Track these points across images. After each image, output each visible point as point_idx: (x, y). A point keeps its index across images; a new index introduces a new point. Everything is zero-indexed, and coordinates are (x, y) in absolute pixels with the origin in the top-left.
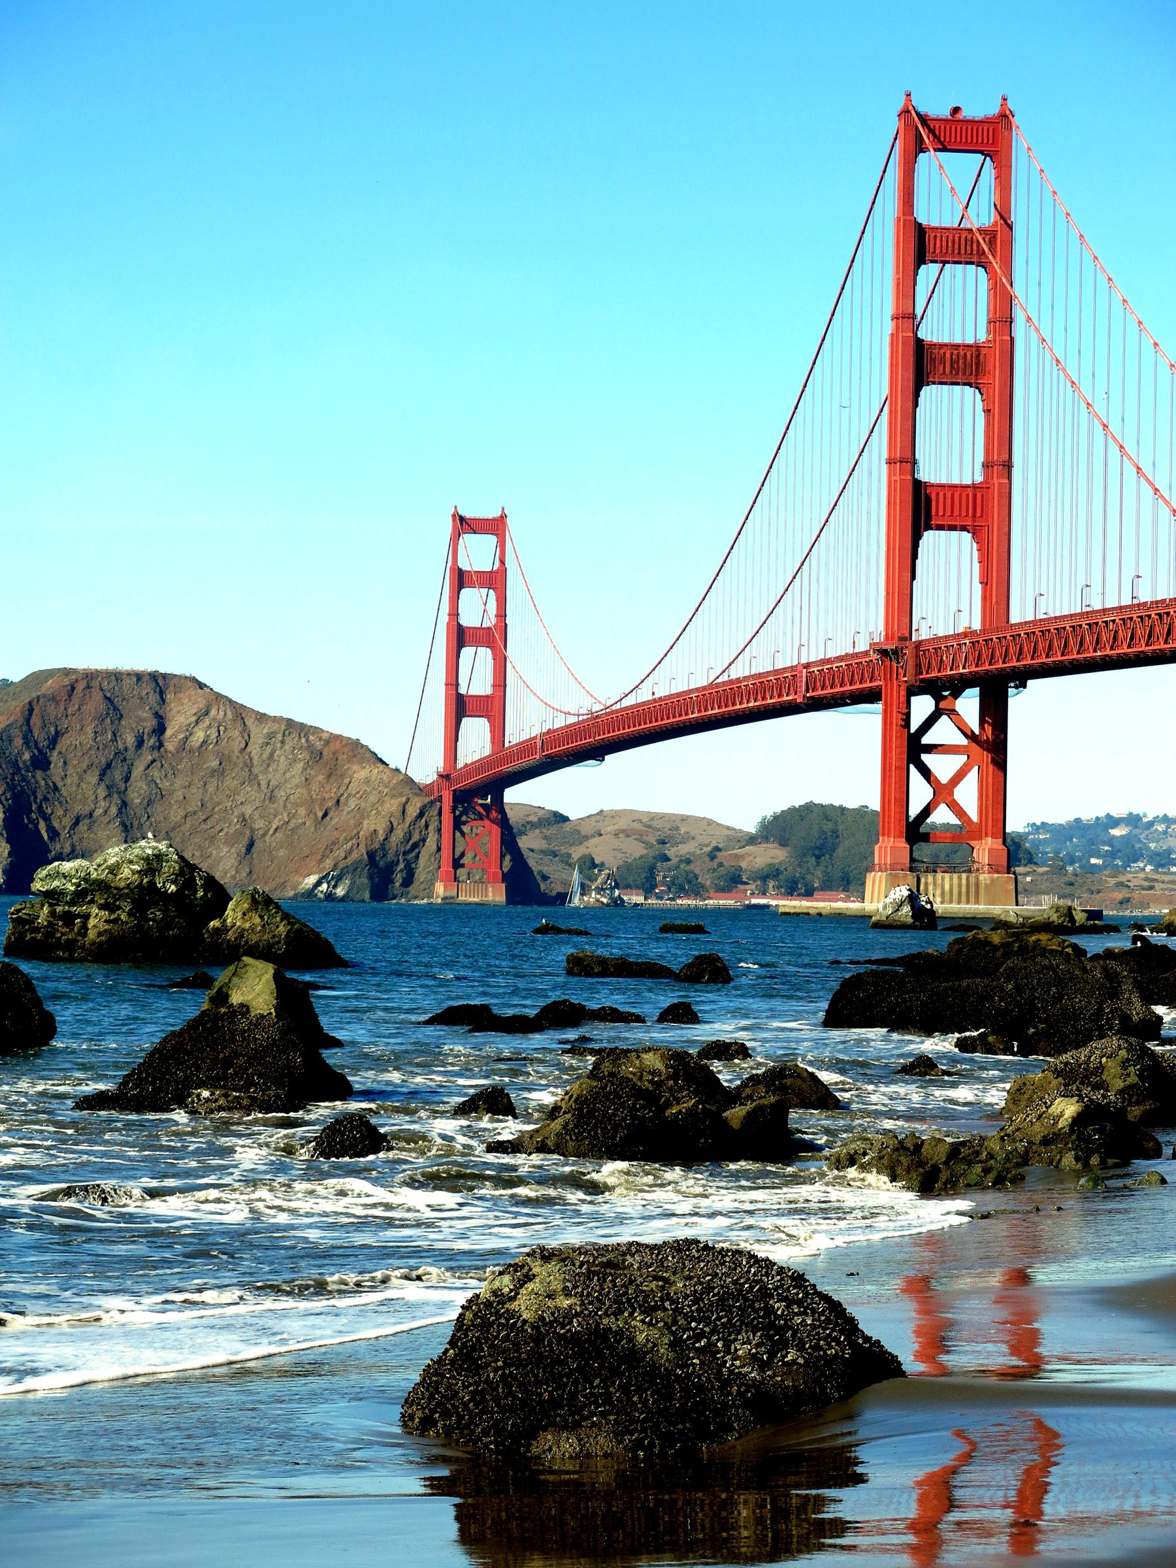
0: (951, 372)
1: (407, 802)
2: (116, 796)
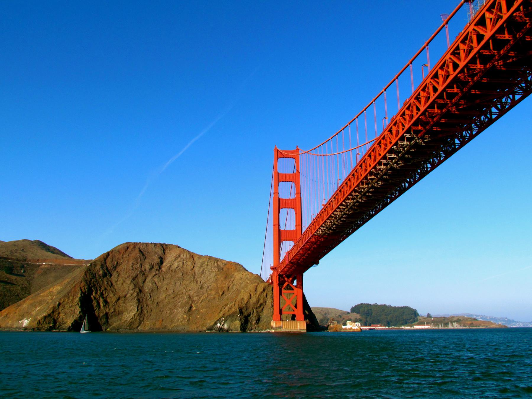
2: (137, 289)
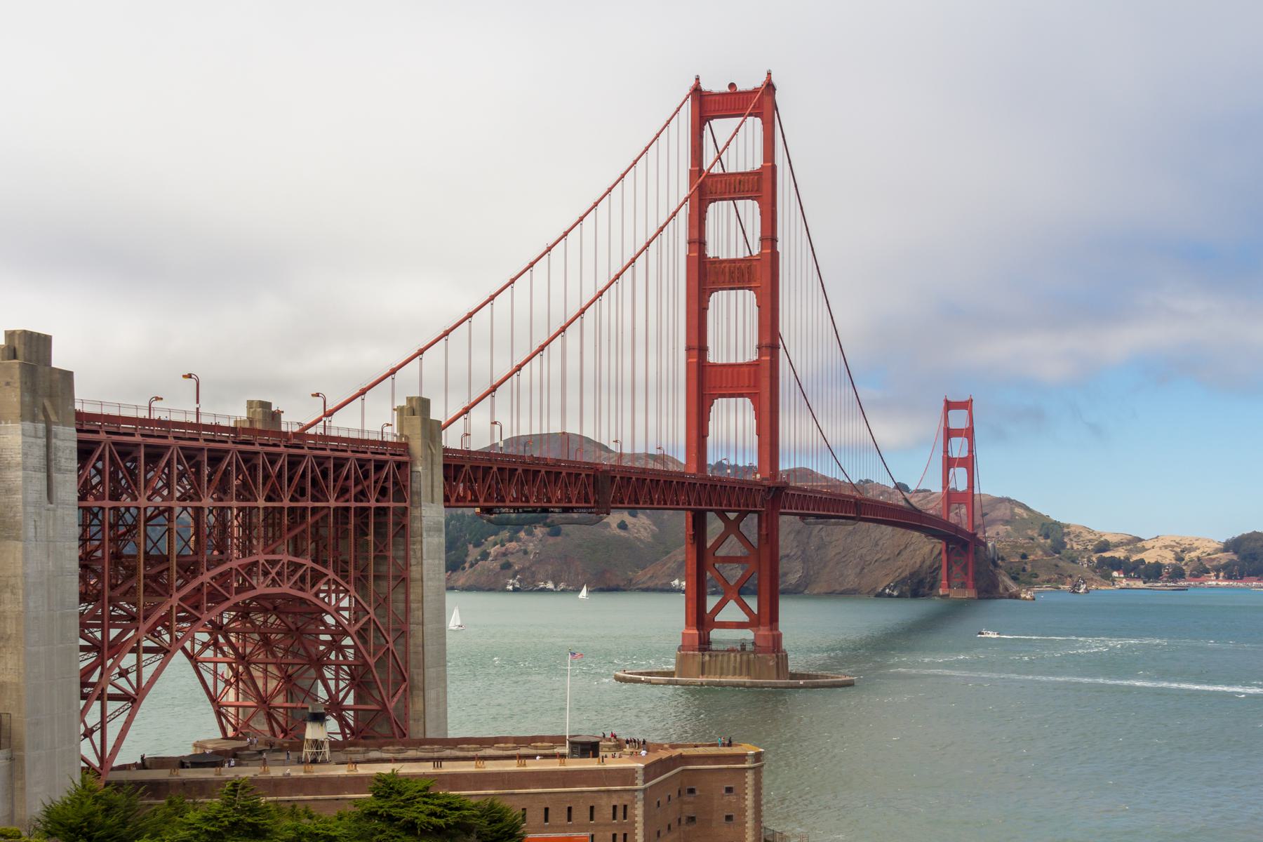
1: (933, 548)
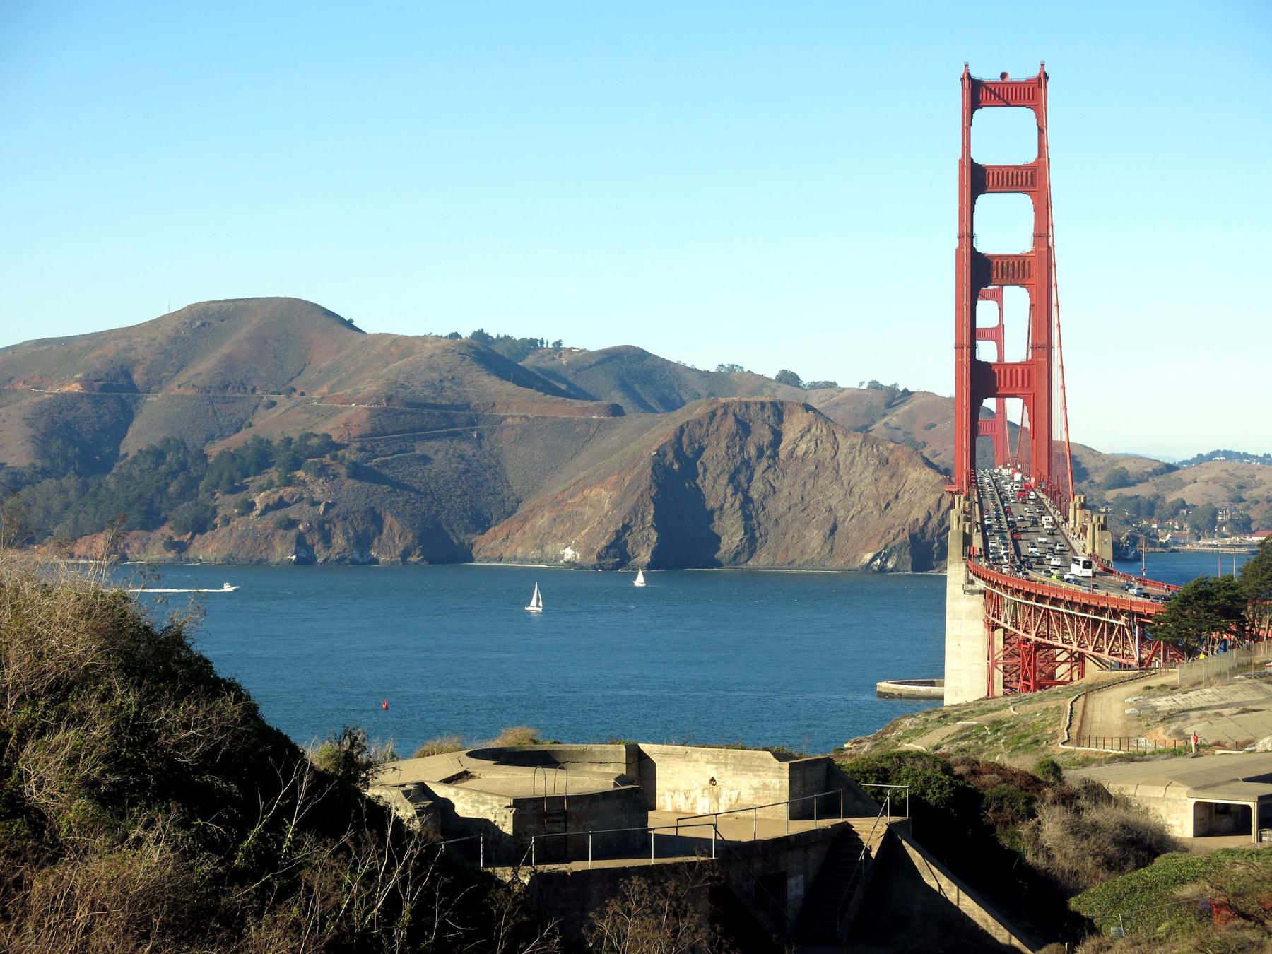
0: (1002, 277)
2: (740, 493)
